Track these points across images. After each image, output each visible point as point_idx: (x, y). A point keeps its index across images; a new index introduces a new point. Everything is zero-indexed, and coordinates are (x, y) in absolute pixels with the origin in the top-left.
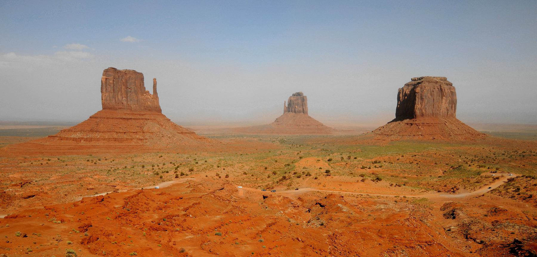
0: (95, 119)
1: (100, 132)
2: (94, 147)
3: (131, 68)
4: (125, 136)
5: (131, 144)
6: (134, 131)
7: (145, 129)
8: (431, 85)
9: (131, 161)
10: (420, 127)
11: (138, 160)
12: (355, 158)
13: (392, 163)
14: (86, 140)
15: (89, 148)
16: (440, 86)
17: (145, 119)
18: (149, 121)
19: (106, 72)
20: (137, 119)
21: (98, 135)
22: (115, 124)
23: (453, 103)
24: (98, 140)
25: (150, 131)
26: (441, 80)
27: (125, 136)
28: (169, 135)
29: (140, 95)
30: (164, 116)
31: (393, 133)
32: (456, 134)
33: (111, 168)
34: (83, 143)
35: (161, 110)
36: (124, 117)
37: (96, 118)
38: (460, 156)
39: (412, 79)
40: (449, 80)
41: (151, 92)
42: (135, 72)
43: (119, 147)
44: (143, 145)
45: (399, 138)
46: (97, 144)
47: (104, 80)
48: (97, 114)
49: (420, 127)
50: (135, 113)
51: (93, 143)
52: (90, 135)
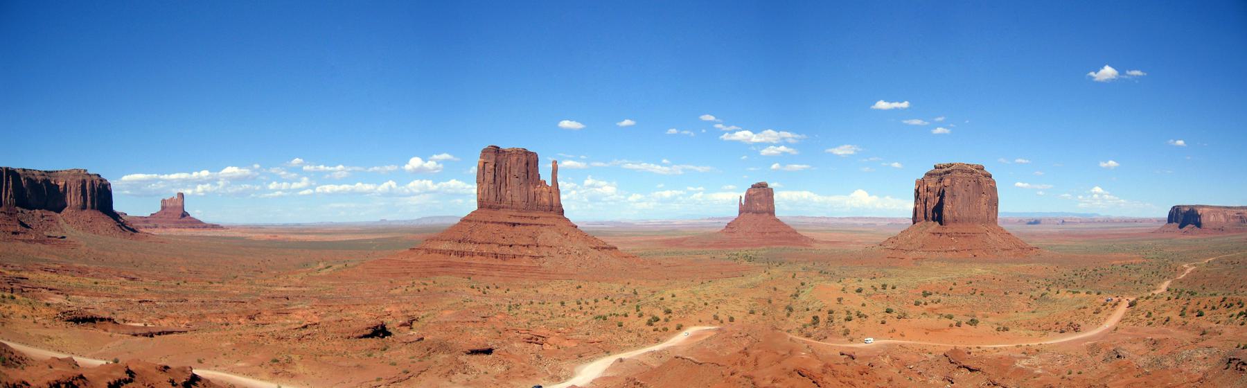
0: (468, 223)
1: (475, 243)
2: (469, 265)
3: (520, 146)
4: (512, 251)
5: (522, 264)
6: (524, 244)
7: (540, 240)
8: (964, 175)
9: (535, 293)
10: (953, 238)
11: (546, 291)
12: (894, 288)
13: (949, 295)
14: (457, 253)
15: (462, 266)
16: (977, 178)
17: (542, 225)
18: (544, 227)
19: (485, 152)
20: (527, 225)
21: (473, 248)
22: (495, 232)
23: (994, 203)
24: (472, 255)
25: (549, 245)
26: (977, 169)
27: (512, 251)
28: (578, 252)
29: (532, 187)
30: (568, 220)
31: (913, 248)
32: (1004, 250)
33: (510, 302)
34: (453, 258)
35: (563, 211)
36: (509, 221)
37: (470, 221)
38: (1028, 281)
39: (936, 167)
40: (988, 169)
41: (549, 183)
42: (526, 153)
43: (504, 267)
44: (540, 267)
45: (924, 255)
46: (471, 260)
47: (482, 165)
48: (471, 215)
49: (953, 238)
50: (524, 214)
51: (466, 259)
52: (462, 247)
